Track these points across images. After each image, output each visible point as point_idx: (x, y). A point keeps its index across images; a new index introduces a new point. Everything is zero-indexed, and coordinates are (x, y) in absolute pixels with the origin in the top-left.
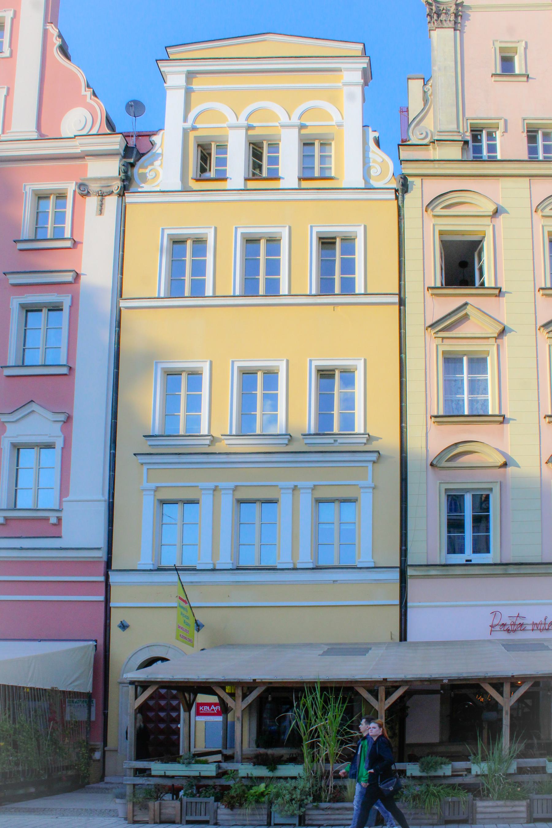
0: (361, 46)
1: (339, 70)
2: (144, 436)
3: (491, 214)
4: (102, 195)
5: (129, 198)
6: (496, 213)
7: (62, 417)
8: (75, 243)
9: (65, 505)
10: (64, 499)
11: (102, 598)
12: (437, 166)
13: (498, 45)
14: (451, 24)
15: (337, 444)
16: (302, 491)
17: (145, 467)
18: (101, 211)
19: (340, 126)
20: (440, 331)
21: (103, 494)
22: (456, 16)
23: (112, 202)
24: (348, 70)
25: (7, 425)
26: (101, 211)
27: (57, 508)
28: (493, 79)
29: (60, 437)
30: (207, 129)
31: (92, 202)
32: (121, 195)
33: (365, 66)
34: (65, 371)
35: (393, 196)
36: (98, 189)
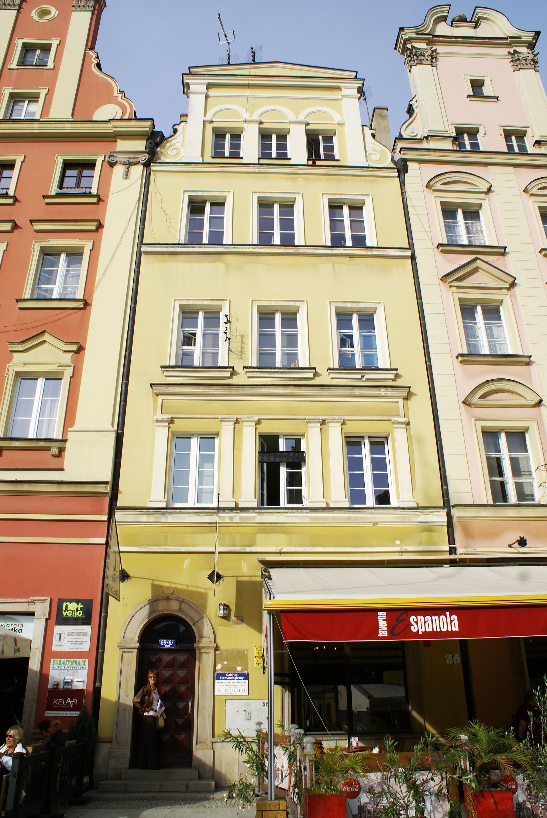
0: (355, 74)
1: (339, 88)
2: (162, 367)
3: (486, 190)
4: (129, 164)
5: (154, 167)
6: (489, 190)
7: (74, 347)
8: (100, 200)
9: (70, 436)
10: (69, 429)
12: (432, 153)
15: (364, 379)
16: (330, 425)
17: (160, 398)
18: (126, 176)
19: (341, 124)
20: (455, 280)
21: (113, 425)
23: (137, 171)
24: (346, 88)
25: (15, 354)
26: (126, 176)
27: (60, 438)
28: (469, 99)
29: (70, 366)
31: (119, 170)
32: (147, 165)
33: (361, 85)
34: (81, 305)
35: (397, 174)
36: (126, 160)
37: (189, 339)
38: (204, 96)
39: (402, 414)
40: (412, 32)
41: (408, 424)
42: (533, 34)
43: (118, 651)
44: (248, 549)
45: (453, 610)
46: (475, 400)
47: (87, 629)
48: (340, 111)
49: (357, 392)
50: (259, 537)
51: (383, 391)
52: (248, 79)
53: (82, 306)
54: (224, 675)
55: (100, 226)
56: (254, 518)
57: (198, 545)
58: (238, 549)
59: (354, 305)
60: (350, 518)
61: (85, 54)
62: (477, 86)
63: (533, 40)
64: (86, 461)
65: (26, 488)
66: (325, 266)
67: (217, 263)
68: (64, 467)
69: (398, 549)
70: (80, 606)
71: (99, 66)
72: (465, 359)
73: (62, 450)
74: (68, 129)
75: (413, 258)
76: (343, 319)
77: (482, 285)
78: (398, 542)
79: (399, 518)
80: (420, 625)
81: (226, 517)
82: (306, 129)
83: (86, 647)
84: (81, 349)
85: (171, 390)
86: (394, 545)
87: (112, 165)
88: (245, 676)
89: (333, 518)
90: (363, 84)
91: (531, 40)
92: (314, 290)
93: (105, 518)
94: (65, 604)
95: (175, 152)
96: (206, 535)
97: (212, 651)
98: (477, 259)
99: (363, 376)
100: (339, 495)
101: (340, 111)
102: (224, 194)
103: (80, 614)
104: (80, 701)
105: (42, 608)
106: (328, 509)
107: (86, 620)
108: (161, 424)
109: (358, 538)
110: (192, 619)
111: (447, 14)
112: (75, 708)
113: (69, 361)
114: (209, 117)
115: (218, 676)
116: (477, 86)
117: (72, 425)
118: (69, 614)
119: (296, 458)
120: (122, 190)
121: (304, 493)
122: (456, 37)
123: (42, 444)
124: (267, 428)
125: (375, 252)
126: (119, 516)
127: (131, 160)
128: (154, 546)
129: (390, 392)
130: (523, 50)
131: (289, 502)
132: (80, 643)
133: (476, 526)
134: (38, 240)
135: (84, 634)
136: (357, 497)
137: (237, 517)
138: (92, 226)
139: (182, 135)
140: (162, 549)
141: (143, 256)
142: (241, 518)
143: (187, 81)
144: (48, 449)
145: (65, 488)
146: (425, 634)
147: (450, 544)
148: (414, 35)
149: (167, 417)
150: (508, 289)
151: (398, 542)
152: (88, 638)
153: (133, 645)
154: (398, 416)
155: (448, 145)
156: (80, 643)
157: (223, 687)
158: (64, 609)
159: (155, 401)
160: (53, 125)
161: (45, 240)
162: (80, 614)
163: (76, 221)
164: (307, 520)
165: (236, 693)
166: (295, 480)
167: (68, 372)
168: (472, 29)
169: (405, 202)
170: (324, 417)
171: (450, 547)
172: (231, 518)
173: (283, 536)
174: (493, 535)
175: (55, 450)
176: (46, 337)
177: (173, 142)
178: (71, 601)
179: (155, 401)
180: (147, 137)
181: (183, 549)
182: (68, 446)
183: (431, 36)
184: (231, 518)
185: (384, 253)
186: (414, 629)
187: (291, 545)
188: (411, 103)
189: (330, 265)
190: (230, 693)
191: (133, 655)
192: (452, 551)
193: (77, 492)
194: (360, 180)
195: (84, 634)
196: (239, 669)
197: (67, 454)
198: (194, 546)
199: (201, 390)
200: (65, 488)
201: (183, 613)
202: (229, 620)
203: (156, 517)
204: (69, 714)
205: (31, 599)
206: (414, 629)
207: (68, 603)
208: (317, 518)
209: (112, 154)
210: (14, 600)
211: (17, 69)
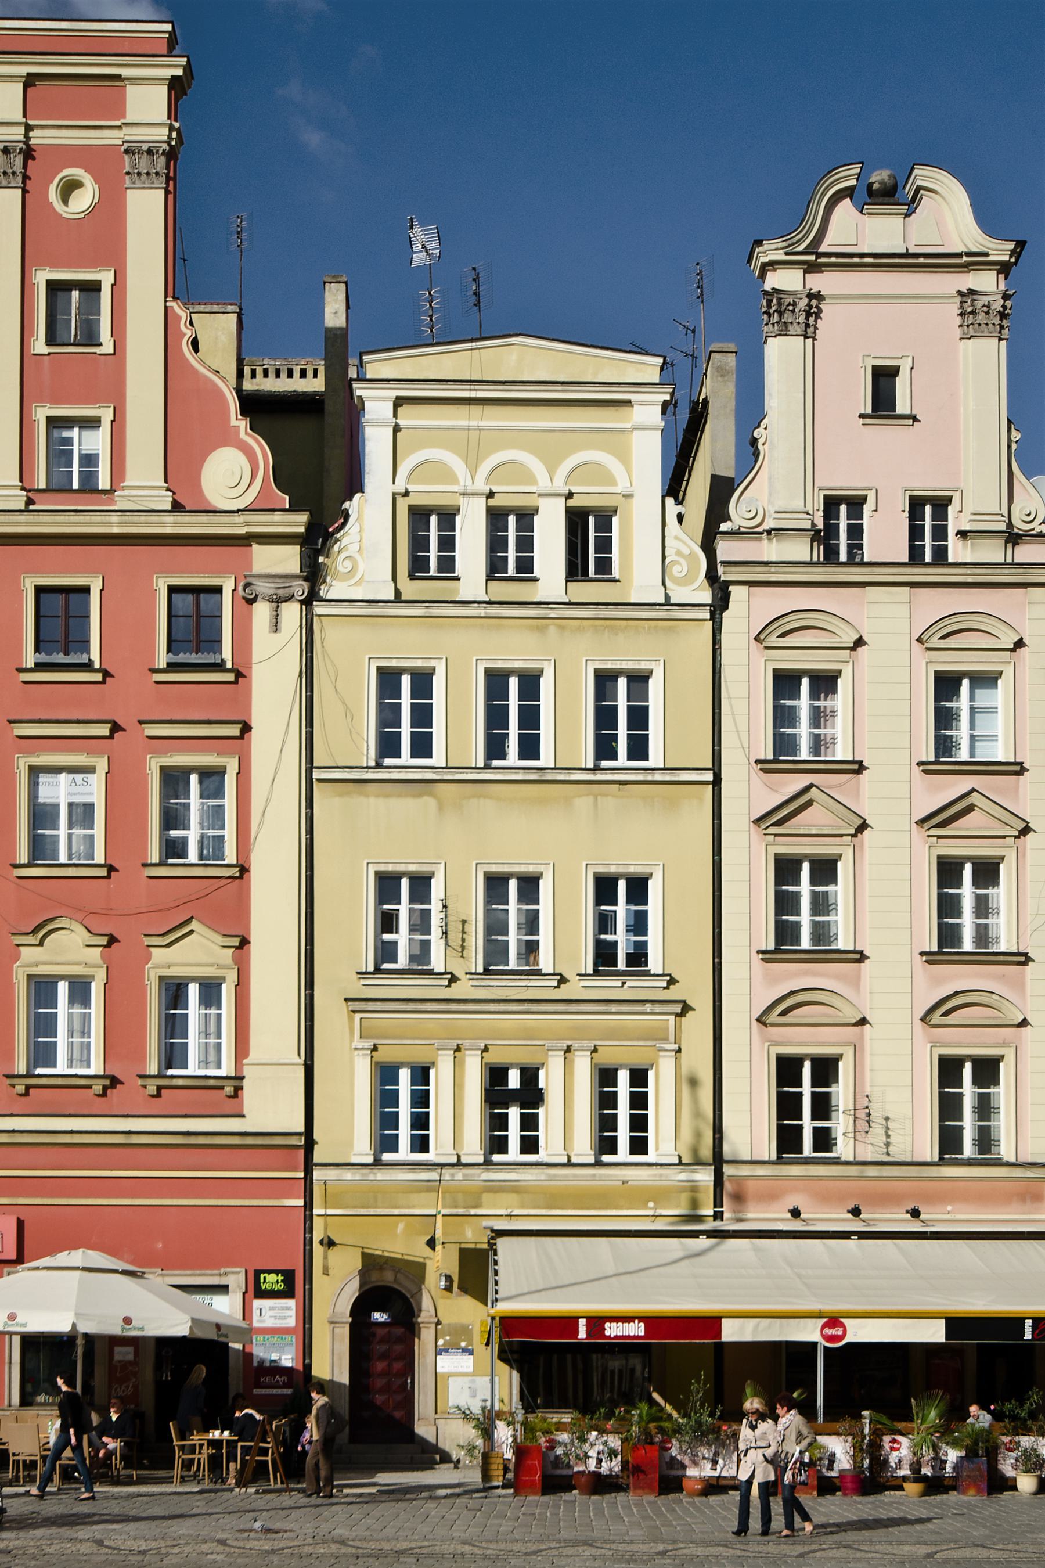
1: (628, 403)
3: (851, 645)
4: (277, 601)
5: (319, 609)
7: (236, 942)
8: (239, 675)
9: (247, 1071)
10: (245, 1061)
11: (301, 1202)
12: (773, 569)
13: (871, 362)
14: (799, 330)
15: (626, 986)
16: (577, 1053)
17: (358, 1016)
18: (276, 627)
19: (628, 496)
21: (299, 1054)
22: (808, 314)
23: (292, 612)
24: (641, 403)
26: (276, 627)
28: (861, 421)
30: (427, 493)
31: (262, 611)
32: (308, 602)
35: (708, 616)
36: (272, 591)
37: (387, 922)
38: (391, 430)
39: (672, 1038)
40: (776, 249)
41: (679, 1051)
42: (1011, 246)
43: (328, 1328)
44: (473, 1212)
45: (641, 1319)
46: (773, 1017)
47: (291, 1303)
48: (625, 459)
49: (614, 1008)
50: (486, 1197)
51: (648, 1007)
52: (468, 387)
53: (238, 875)
54: (447, 1351)
55: (246, 728)
56: (479, 1175)
57: (413, 1207)
58: (461, 1211)
59: (622, 870)
60: (594, 1175)
61: (166, 308)
62: (884, 378)
63: (1011, 257)
64: (271, 1106)
65: (202, 1140)
66: (583, 802)
67: (425, 798)
68: (245, 1112)
69: (651, 1213)
70: (280, 1278)
71: (195, 344)
72: (768, 956)
73: (238, 1089)
74: (171, 524)
75: (717, 782)
76: (605, 888)
77: (814, 832)
78: (651, 1204)
79: (655, 1175)
80: (612, 1330)
81: (447, 1174)
82: (566, 507)
83: (291, 1322)
84: (244, 942)
85: (371, 1006)
86: (646, 1207)
87: (251, 602)
88: (471, 1353)
89: (575, 1175)
90: (672, 394)
91: (1007, 258)
92: (566, 842)
93: (301, 1175)
94: (262, 1276)
95: (348, 564)
96: (423, 1194)
97: (433, 1326)
98: (811, 786)
99: (624, 983)
100: (583, 1147)
101: (625, 459)
102: (432, 663)
103: (281, 1286)
104: (290, 1379)
105: (236, 1280)
106: (569, 1164)
107: (288, 1293)
108: (361, 1052)
109: (602, 1198)
110: (409, 1291)
111: (854, 182)
112: (285, 1386)
113: (229, 961)
114: (400, 487)
115: (438, 1352)
116: (884, 378)
117: (246, 1055)
118: (268, 1287)
119: (531, 1095)
120: (271, 650)
121: (542, 1142)
122: (862, 255)
123: (212, 1082)
124: (495, 1057)
125: (658, 776)
126: (318, 1174)
127: (281, 592)
128: (363, 1207)
129: (658, 1008)
130: (987, 282)
131: (523, 1151)
132: (285, 1318)
133: (751, 1186)
134: (157, 753)
135: (288, 1308)
136: (607, 1145)
137: (459, 1174)
138: (235, 731)
139: (357, 524)
140: (372, 1211)
141: (316, 786)
142: (464, 1175)
143: (358, 393)
144: (222, 1088)
145: (250, 1141)
146: (616, 1337)
147: (715, 1206)
148: (780, 256)
149: (369, 1044)
150: (852, 836)
151: (651, 1204)
152: (293, 1313)
153: (344, 1320)
154: (666, 1039)
155: (800, 549)
156: (285, 1318)
157: (446, 1364)
158: (262, 1280)
159: (351, 1020)
160: (143, 518)
161: (164, 753)
162: (281, 1286)
163: (209, 722)
164: (543, 1178)
165: (460, 1370)
166: (529, 1123)
167: (232, 977)
168: (900, 220)
169: (717, 670)
170: (569, 1043)
171: (715, 1212)
172: (453, 1175)
173: (514, 1195)
174: (770, 1197)
175: (229, 1090)
176: (194, 925)
177: (345, 541)
178: (269, 1272)
179: (351, 1020)
180: (301, 540)
181: (396, 1212)
182: (245, 1083)
183: (813, 257)
184: (453, 1175)
185: (671, 777)
186: (607, 1333)
187: (523, 1207)
188: (756, 434)
189: (591, 799)
190: (453, 1370)
191: (346, 1330)
192: (718, 1216)
193: (263, 1144)
194: (649, 627)
195: (288, 1308)
196: (463, 1344)
197: (247, 1093)
198: (409, 1207)
199: (411, 1006)
200: (250, 1141)
201: (400, 1284)
202: (451, 1292)
203: (363, 1175)
204: (279, 1391)
205: (222, 1271)
206: (607, 1333)
207: (266, 1275)
208: (555, 1175)
209: (249, 580)
210: (203, 1272)
211: (49, 354)
